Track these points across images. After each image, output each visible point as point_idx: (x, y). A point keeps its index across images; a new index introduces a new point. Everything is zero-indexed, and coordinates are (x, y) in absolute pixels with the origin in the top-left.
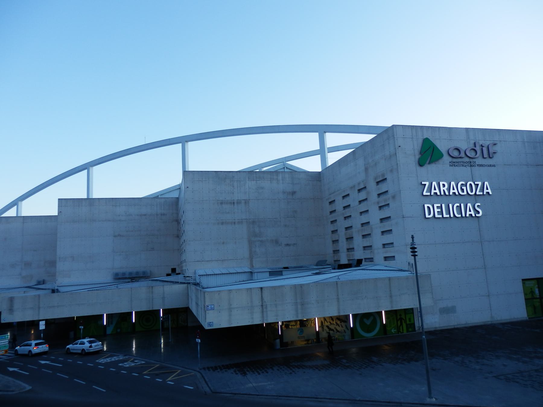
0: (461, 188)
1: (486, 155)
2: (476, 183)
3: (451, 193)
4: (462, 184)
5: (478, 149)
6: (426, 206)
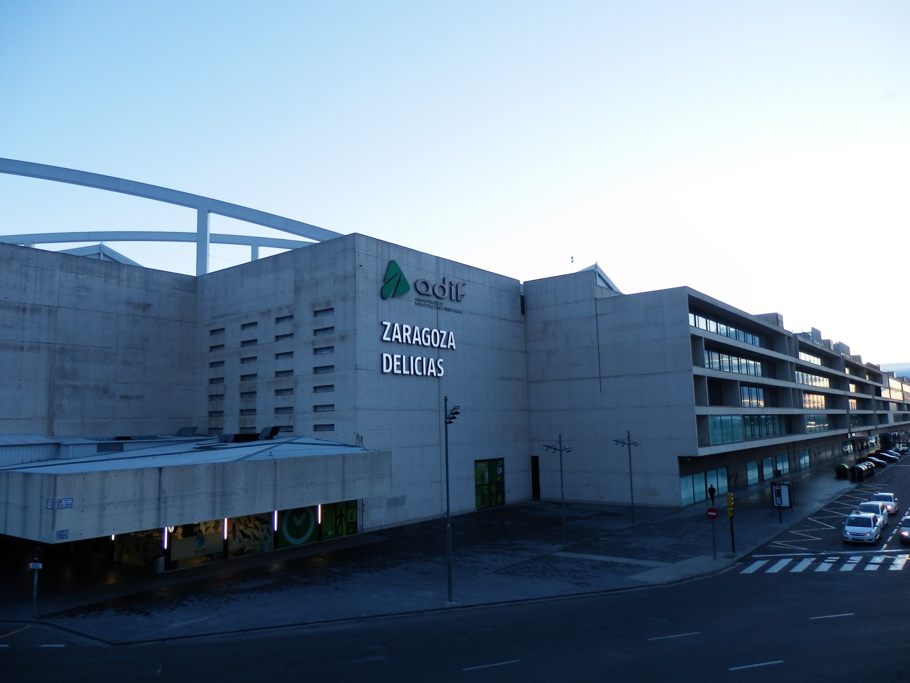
0: (425, 336)
1: (454, 298)
2: (441, 332)
3: (414, 343)
4: (427, 331)
5: (447, 286)
6: (385, 355)
